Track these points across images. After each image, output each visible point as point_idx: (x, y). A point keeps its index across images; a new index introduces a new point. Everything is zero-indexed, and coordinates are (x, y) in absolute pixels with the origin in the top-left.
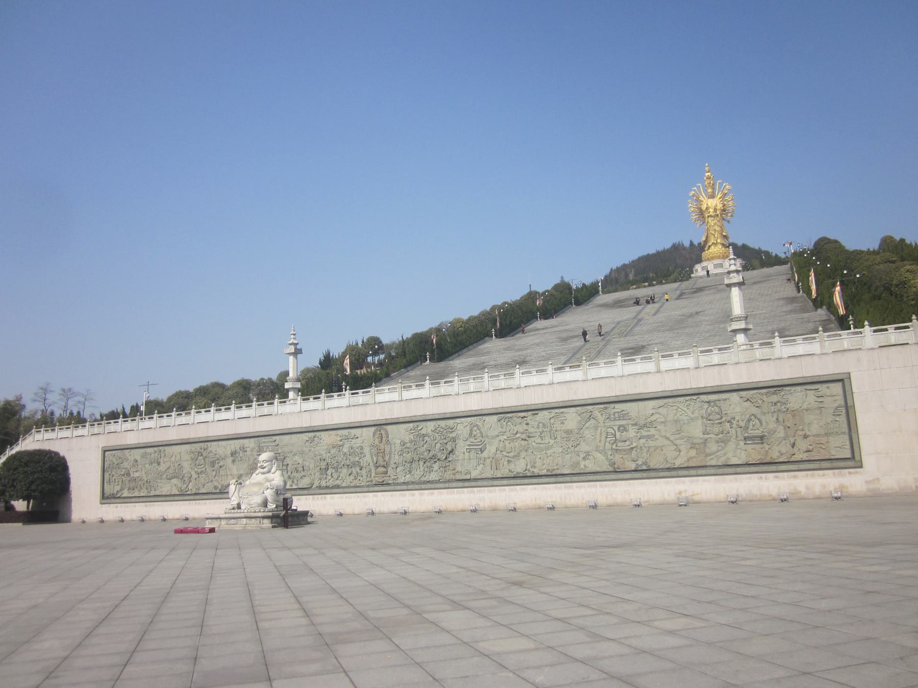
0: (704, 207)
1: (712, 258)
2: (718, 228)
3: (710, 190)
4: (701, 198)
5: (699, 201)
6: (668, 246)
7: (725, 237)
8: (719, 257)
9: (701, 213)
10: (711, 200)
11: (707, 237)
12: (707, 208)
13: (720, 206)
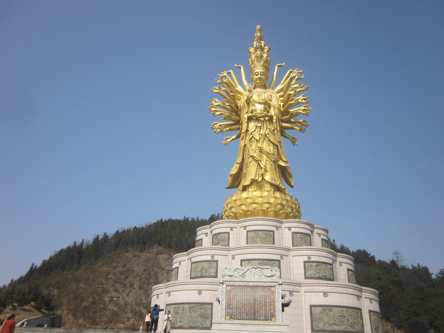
0: (241, 103)
1: (246, 214)
2: (267, 147)
3: (259, 69)
4: (239, 88)
8: (265, 213)
11: (241, 169)
12: (248, 102)
13: (276, 102)
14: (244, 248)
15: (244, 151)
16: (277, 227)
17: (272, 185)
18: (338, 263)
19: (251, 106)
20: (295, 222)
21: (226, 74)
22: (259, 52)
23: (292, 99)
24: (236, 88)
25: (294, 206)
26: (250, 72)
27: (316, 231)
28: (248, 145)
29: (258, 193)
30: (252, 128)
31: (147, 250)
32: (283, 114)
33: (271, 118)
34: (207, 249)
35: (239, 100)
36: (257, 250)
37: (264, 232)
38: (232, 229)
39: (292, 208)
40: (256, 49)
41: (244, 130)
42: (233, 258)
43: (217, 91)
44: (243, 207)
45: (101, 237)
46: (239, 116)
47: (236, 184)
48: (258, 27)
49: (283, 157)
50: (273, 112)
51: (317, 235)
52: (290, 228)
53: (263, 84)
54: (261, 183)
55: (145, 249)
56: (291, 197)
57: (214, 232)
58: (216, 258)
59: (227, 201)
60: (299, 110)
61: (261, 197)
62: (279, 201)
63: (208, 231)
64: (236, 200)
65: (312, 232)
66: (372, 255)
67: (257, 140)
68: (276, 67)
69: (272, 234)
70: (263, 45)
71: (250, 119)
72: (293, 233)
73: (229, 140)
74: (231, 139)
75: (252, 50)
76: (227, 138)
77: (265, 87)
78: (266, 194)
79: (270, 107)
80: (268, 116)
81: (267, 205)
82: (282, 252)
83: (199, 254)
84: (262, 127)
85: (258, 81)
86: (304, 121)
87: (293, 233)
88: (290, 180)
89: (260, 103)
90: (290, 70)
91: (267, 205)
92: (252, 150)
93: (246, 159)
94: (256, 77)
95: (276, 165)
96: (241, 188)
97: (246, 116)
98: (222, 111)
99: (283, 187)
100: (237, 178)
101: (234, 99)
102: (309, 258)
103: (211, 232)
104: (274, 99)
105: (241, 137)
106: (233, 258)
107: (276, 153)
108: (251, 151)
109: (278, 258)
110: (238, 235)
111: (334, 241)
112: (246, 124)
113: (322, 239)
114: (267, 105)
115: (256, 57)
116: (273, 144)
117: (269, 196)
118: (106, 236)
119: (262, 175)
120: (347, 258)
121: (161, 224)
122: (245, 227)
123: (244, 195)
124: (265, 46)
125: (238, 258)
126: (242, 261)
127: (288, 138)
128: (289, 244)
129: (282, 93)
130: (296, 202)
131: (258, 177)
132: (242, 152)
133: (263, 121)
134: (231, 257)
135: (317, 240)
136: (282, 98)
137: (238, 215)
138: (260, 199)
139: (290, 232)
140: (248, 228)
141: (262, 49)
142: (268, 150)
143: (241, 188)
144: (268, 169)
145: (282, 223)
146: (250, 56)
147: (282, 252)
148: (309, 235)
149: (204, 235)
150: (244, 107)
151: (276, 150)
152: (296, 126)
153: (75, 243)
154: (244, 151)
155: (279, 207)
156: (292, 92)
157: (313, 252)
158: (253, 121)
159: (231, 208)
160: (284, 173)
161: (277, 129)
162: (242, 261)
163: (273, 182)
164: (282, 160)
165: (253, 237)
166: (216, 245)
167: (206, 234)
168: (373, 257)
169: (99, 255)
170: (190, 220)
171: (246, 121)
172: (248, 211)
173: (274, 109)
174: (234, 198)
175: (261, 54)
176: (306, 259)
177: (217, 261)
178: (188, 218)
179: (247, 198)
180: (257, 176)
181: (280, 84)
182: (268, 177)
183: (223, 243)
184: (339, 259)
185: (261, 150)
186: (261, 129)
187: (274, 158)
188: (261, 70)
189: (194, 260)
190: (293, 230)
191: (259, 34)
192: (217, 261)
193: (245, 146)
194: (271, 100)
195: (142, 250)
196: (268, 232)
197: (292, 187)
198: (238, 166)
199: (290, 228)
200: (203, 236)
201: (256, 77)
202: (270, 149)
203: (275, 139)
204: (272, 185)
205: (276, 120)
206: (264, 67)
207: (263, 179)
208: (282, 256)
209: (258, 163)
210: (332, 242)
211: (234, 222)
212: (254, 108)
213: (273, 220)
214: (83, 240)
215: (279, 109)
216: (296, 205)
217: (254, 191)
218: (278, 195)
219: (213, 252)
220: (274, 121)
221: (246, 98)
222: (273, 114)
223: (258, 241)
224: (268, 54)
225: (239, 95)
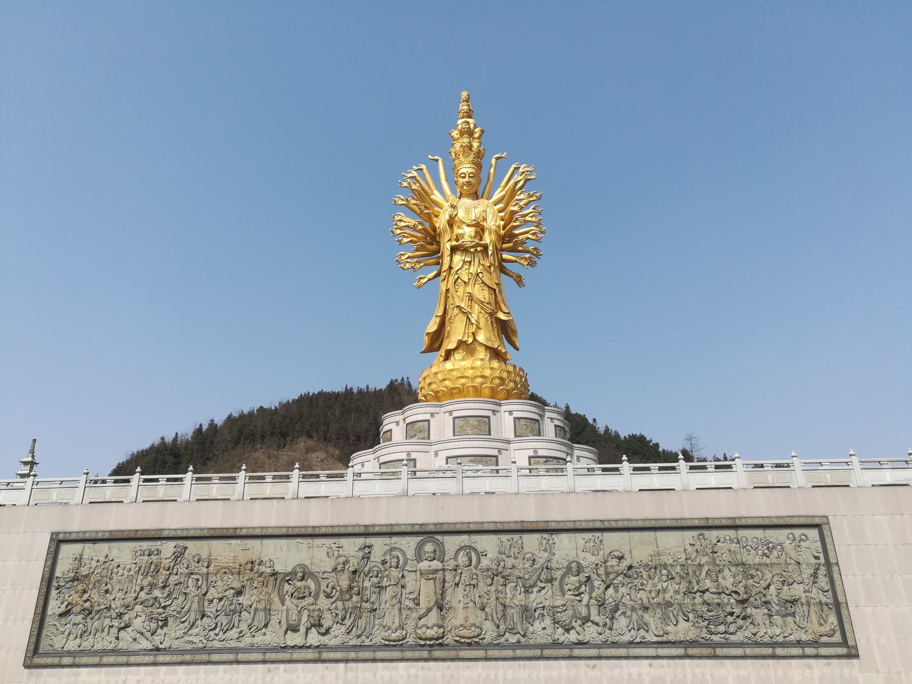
0: (441, 222)
1: (454, 393)
2: (481, 294)
3: (466, 168)
4: (437, 196)
5: (423, 195)
6: (380, 383)
7: (505, 329)
8: (477, 391)
9: (430, 242)
10: (466, 201)
11: (442, 325)
12: (451, 223)
13: (493, 222)
14: (450, 441)
15: (447, 298)
16: (493, 411)
17: (487, 348)
18: (575, 458)
19: (455, 228)
20: (518, 404)
21: (415, 174)
22: (466, 140)
23: (517, 219)
24: (432, 197)
25: (518, 379)
26: (452, 171)
27: (548, 414)
28: (452, 290)
29: (467, 363)
30: (457, 264)
31: (288, 446)
32: (503, 239)
33: (486, 247)
34: (401, 444)
35: (437, 216)
36: (467, 444)
37: (477, 419)
39: (515, 382)
40: (462, 133)
41: (445, 267)
42: (436, 454)
43: (403, 202)
44: (447, 383)
45: (205, 428)
46: (438, 243)
47: (436, 345)
48: (464, 94)
49: (503, 306)
50: (488, 239)
52: (511, 412)
53: (473, 191)
54: (473, 346)
55: (285, 445)
56: (514, 366)
57: (408, 420)
58: (413, 456)
59: (424, 374)
60: (527, 232)
61: (472, 368)
62: (497, 374)
63: (400, 418)
64: (436, 373)
65: (542, 416)
66: (654, 441)
67: (465, 282)
68: (493, 161)
70: (472, 126)
71: (454, 250)
72: (515, 419)
73: (423, 281)
74: (426, 279)
75: (455, 134)
76: (421, 278)
77: (476, 196)
78: (479, 363)
79: (483, 230)
80: (481, 245)
81: (480, 380)
82: (500, 445)
83: (386, 452)
85: (465, 187)
86: (535, 249)
87: (515, 419)
88: (514, 338)
89: (468, 225)
90: (514, 166)
91: (480, 380)
92: (459, 297)
93: (450, 311)
94: (461, 180)
96: (442, 352)
97: (448, 246)
98: (412, 236)
99: (503, 351)
100: (436, 340)
101: (429, 218)
102: (535, 451)
103: (404, 420)
104: (490, 217)
105: (442, 277)
106: (436, 454)
107: (493, 301)
108: (456, 299)
109: (495, 452)
110: (442, 424)
111: (595, 420)
113: (556, 426)
114: (480, 229)
115: (461, 146)
116: (489, 287)
117: (483, 367)
118: (212, 425)
119: (473, 334)
120: (587, 450)
121: (308, 402)
122: (451, 412)
123: (449, 365)
124: (475, 127)
125: (443, 455)
126: (448, 458)
127: (511, 277)
128: (509, 434)
129: (501, 205)
130: (521, 373)
132: (443, 299)
133: (474, 253)
134: (433, 453)
135: (549, 428)
136: (502, 214)
137: (440, 394)
138: (471, 371)
140: (455, 414)
141: (470, 133)
142: (481, 297)
143: (442, 352)
144: (481, 326)
145: (500, 405)
146: (453, 144)
147: (500, 445)
148: (538, 421)
149: (394, 423)
150: (445, 230)
152: (522, 259)
153: (163, 438)
154: (447, 298)
155: (497, 381)
156: (516, 208)
157: (540, 445)
158: (458, 253)
159: (430, 384)
160: (505, 329)
161: (494, 265)
162: (448, 458)
163: (489, 344)
164: (501, 310)
165: (461, 426)
166: (411, 437)
167: (397, 423)
168: (657, 445)
169: (208, 459)
170: (355, 391)
171: (449, 253)
172: (454, 389)
174: (434, 370)
175: (470, 142)
176: (531, 453)
177: (414, 460)
178: (351, 389)
179: (452, 370)
181: (500, 189)
182: (481, 337)
183: (421, 436)
184: (577, 453)
185: (471, 298)
186: (470, 264)
187: (489, 308)
188: (470, 170)
189: (382, 460)
190: (516, 414)
191: (465, 108)
192: (414, 460)
193: (447, 290)
194: (485, 219)
195: (279, 448)
197: (517, 349)
198: (438, 320)
199: (511, 412)
200: (392, 426)
201: (461, 180)
203: (491, 279)
204: (487, 348)
205: (493, 251)
206: (474, 163)
207: (475, 340)
208: (500, 450)
209: (468, 317)
210: (591, 422)
211: (436, 406)
212: (460, 231)
213: (488, 402)
214: (177, 434)
215: (498, 235)
216: (521, 377)
217: (463, 359)
218: (495, 364)
219: (409, 448)
220: (490, 253)
221: (447, 217)
222: (488, 241)
223: (470, 432)
224: (480, 142)
225: (436, 209)
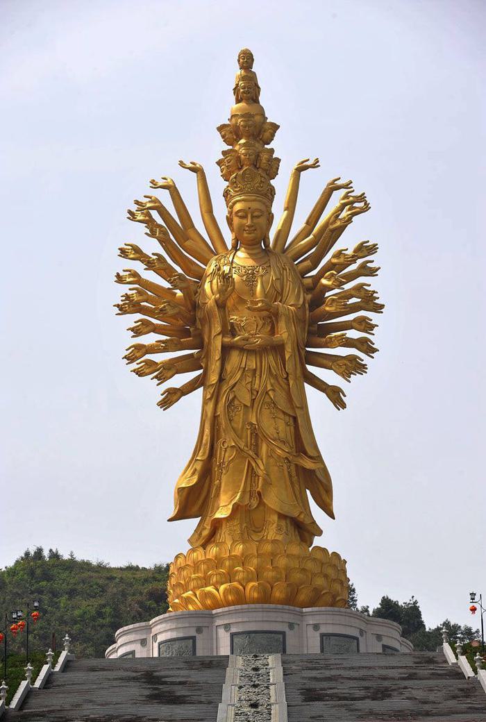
16: (291, 626)
17: (282, 516)
37: (266, 636)
38: (199, 630)
51: (374, 637)
67: (245, 406)
69: (281, 640)
72: (322, 636)
84: (258, 373)
87: (322, 636)
95: (293, 468)
97: (217, 343)
107: (291, 438)
112: (218, 364)
116: (284, 413)
131: (251, 496)
139: (317, 634)
151: (292, 428)
173: (287, 322)
180: (247, 496)
190: (323, 630)
193: (215, 417)
196: (273, 635)
199: (316, 627)
202: (276, 429)
204: (282, 516)
207: (261, 503)
222: (285, 336)
